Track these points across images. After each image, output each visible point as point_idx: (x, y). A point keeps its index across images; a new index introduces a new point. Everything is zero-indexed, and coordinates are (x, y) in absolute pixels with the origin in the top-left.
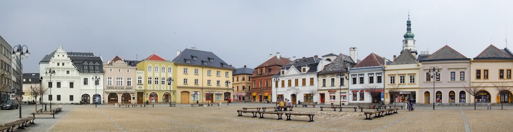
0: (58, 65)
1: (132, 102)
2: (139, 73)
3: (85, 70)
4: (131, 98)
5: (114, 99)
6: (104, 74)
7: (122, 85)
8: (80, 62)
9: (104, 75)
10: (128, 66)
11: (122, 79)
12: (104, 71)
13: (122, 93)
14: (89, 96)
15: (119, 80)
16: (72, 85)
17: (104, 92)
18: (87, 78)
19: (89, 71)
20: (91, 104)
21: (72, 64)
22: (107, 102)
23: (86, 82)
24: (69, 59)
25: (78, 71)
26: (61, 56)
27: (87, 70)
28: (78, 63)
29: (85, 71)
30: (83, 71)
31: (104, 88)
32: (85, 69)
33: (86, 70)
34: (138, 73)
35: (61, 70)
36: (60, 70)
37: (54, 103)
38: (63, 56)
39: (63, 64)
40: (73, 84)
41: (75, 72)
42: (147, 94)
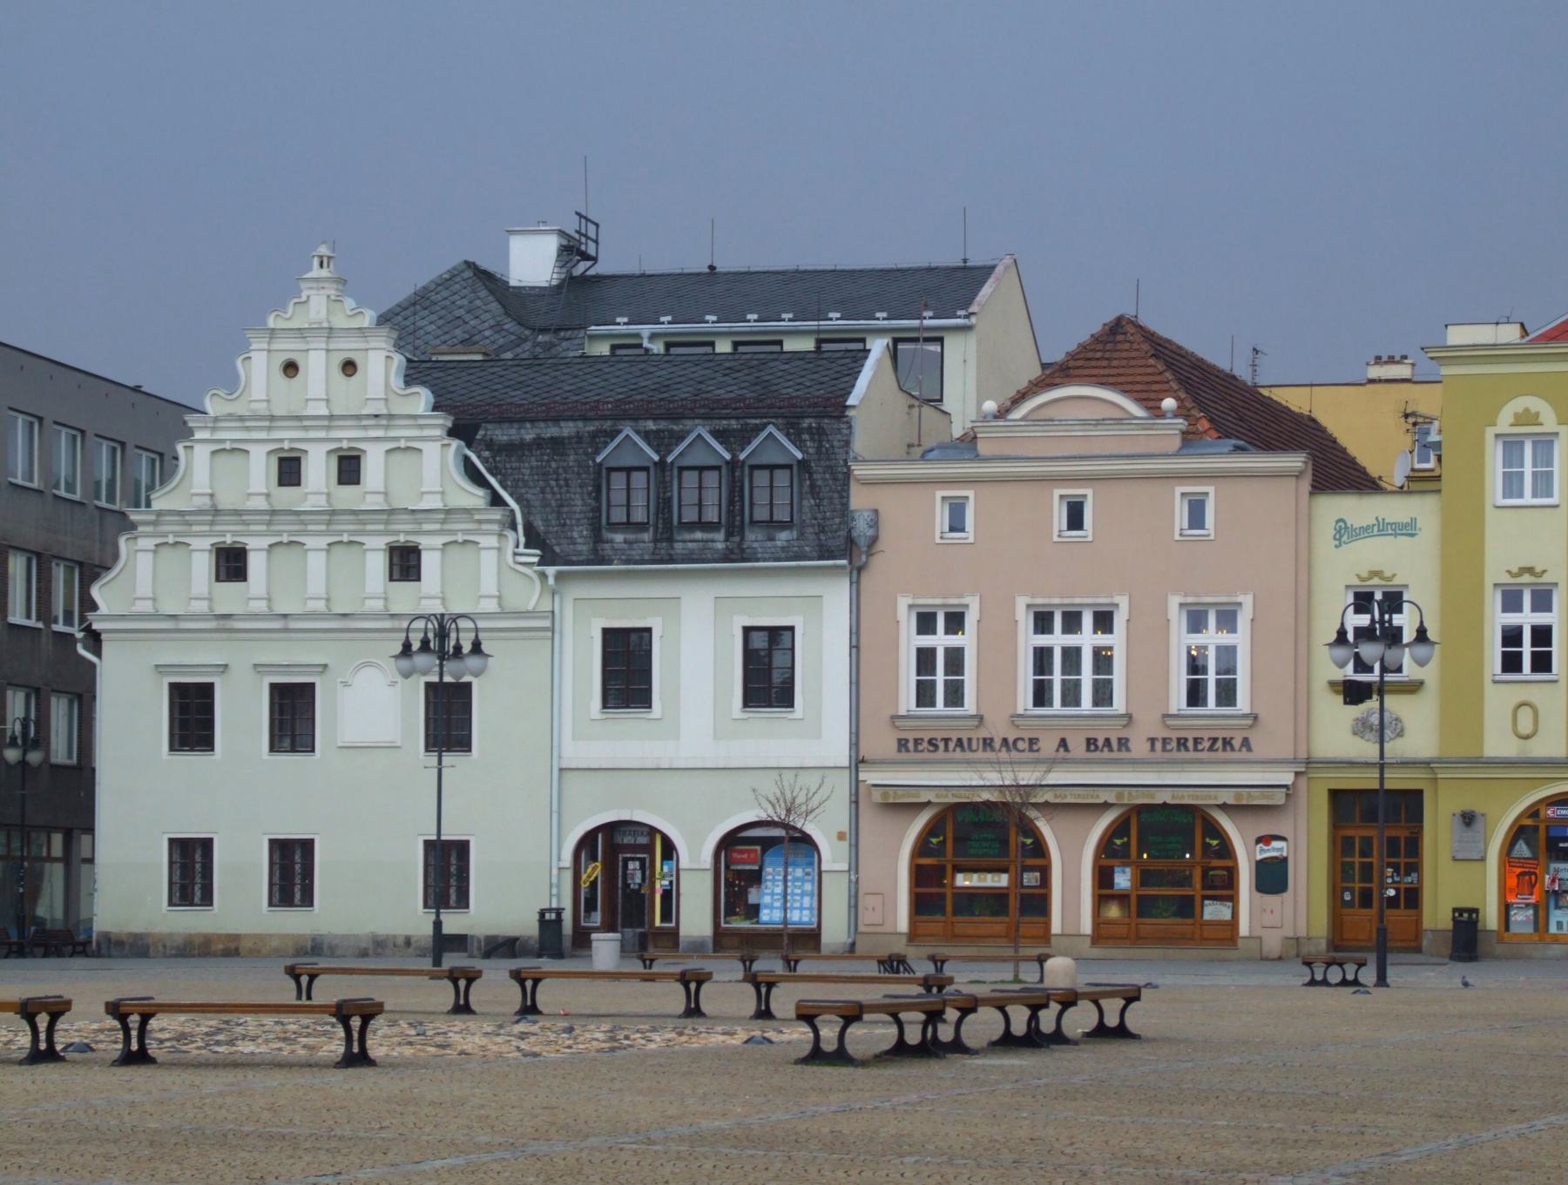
0: (343, 480)
1: (1244, 929)
2: (1365, 532)
3: (614, 527)
4: (1232, 873)
5: (1002, 880)
6: (857, 572)
7: (1103, 694)
8: (567, 429)
9: (856, 585)
10: (1189, 439)
11: (1104, 621)
12: (861, 527)
13: (1106, 806)
14: (669, 850)
15: (1071, 640)
17: (855, 801)
18: (791, 629)
22: (903, 924)
24: (421, 399)
25: (533, 539)
26: (317, 365)
27: (642, 527)
28: (539, 443)
29: (619, 538)
30: (597, 537)
31: (855, 744)
32: (618, 515)
33: (629, 525)
34: (1344, 532)
35: (323, 542)
36: (310, 542)
37: (236, 938)
38: (349, 367)
39: (349, 468)
40: (209, 709)
41: (489, 560)
42: (1468, 819)
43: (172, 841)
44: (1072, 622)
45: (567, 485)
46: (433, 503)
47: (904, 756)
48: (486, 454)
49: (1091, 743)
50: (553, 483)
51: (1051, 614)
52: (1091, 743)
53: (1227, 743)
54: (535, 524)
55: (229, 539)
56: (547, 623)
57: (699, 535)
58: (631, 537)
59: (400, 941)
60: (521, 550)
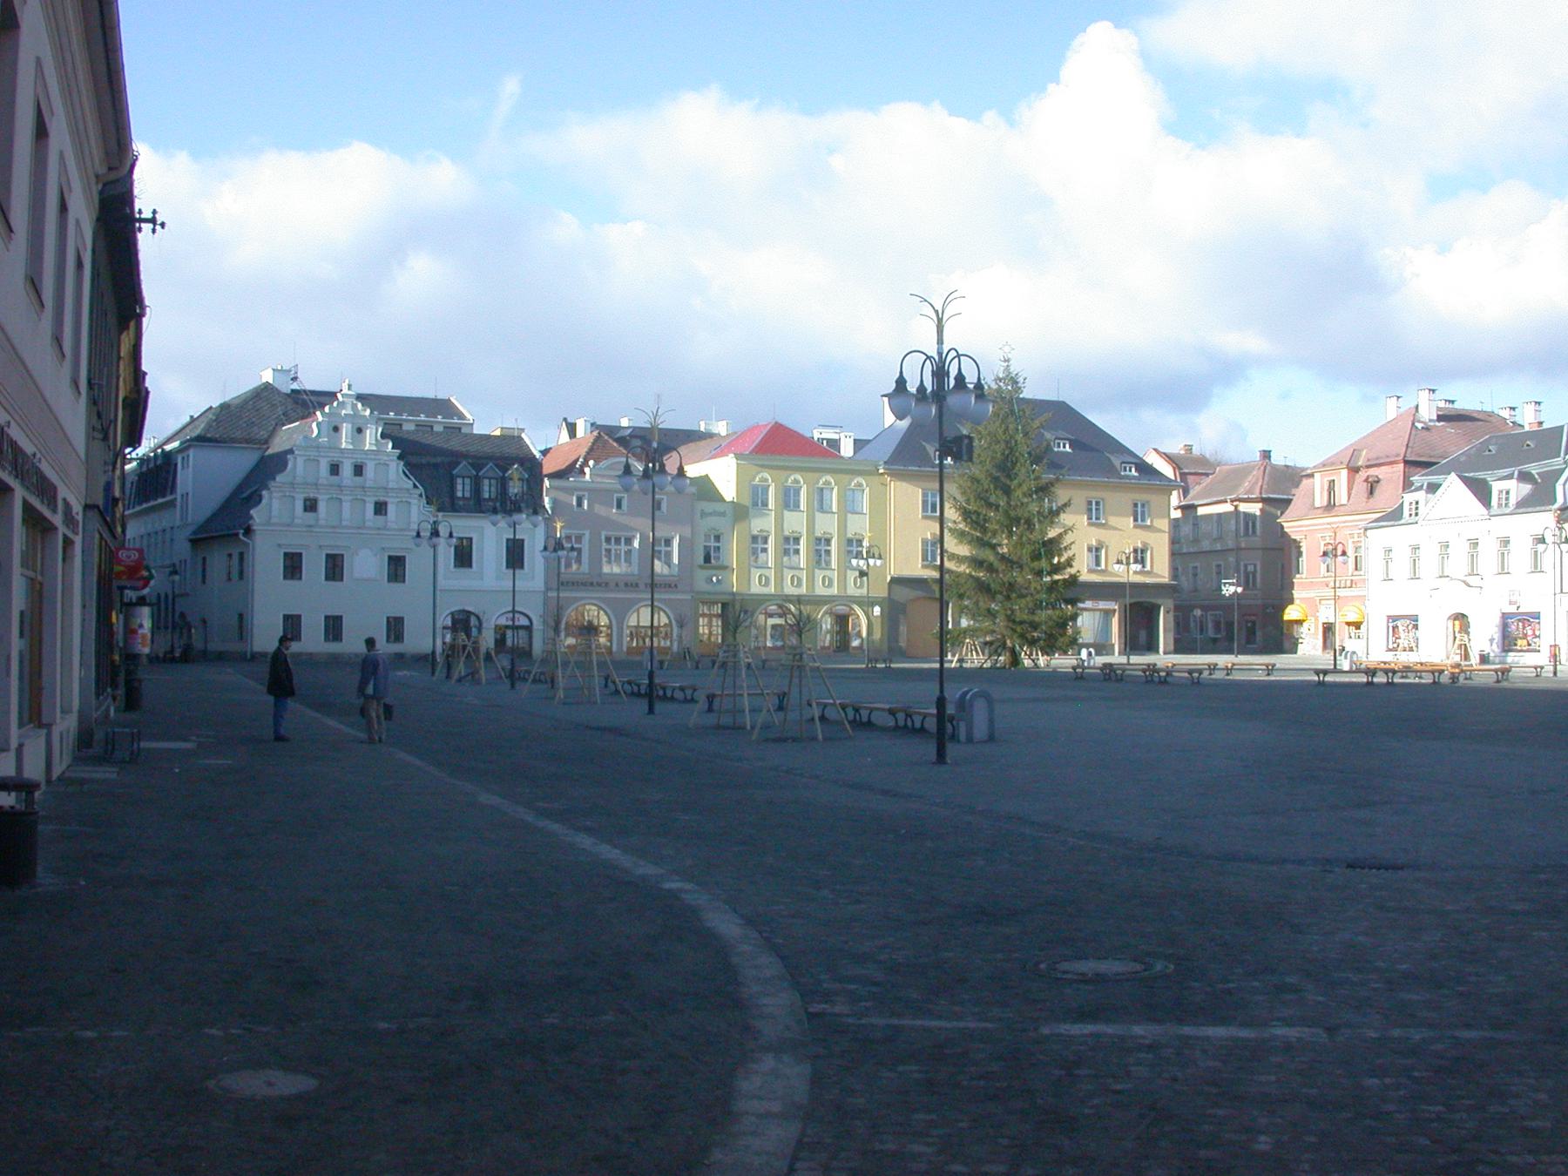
2: (711, 514)
16: (397, 567)
19: (477, 505)
23: (464, 556)
29: (461, 503)
31: (546, 583)
34: (704, 514)
39: (359, 470)
41: (414, 510)
44: (618, 540)
49: (626, 585)
51: (620, 538)
52: (626, 585)
53: (670, 586)
55: (312, 495)
60: (426, 505)
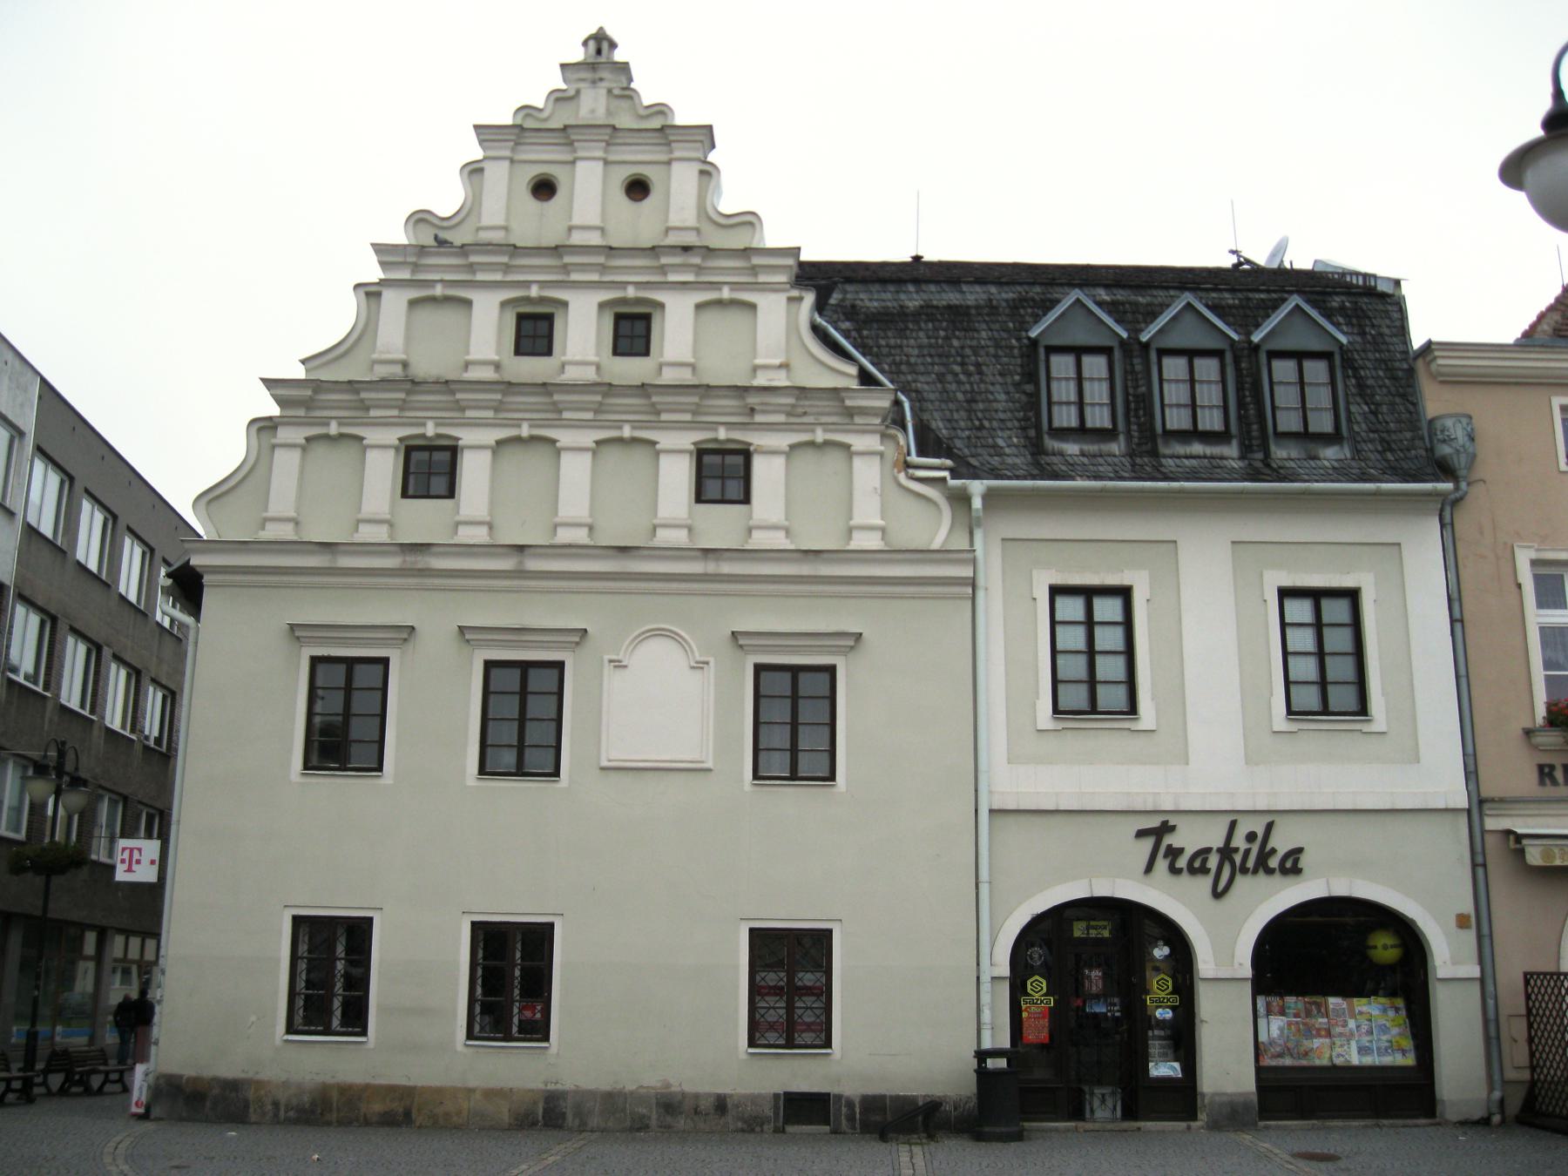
3: (1063, 433)
17: (1478, 864)
20: (1232, 1117)
21: (816, 329)
25: (928, 443)
28: (928, 312)
29: (1072, 448)
30: (1036, 448)
31: (1472, 774)
32: (1066, 417)
33: (1082, 431)
35: (588, 438)
36: (565, 437)
41: (868, 475)
43: (297, 921)
45: (980, 373)
46: (780, 380)
47: (1549, 791)
48: (847, 325)
50: (957, 369)
54: (934, 425)
56: (967, 572)
57: (1197, 448)
58: (1092, 448)
59: (705, 1105)
60: (914, 458)
